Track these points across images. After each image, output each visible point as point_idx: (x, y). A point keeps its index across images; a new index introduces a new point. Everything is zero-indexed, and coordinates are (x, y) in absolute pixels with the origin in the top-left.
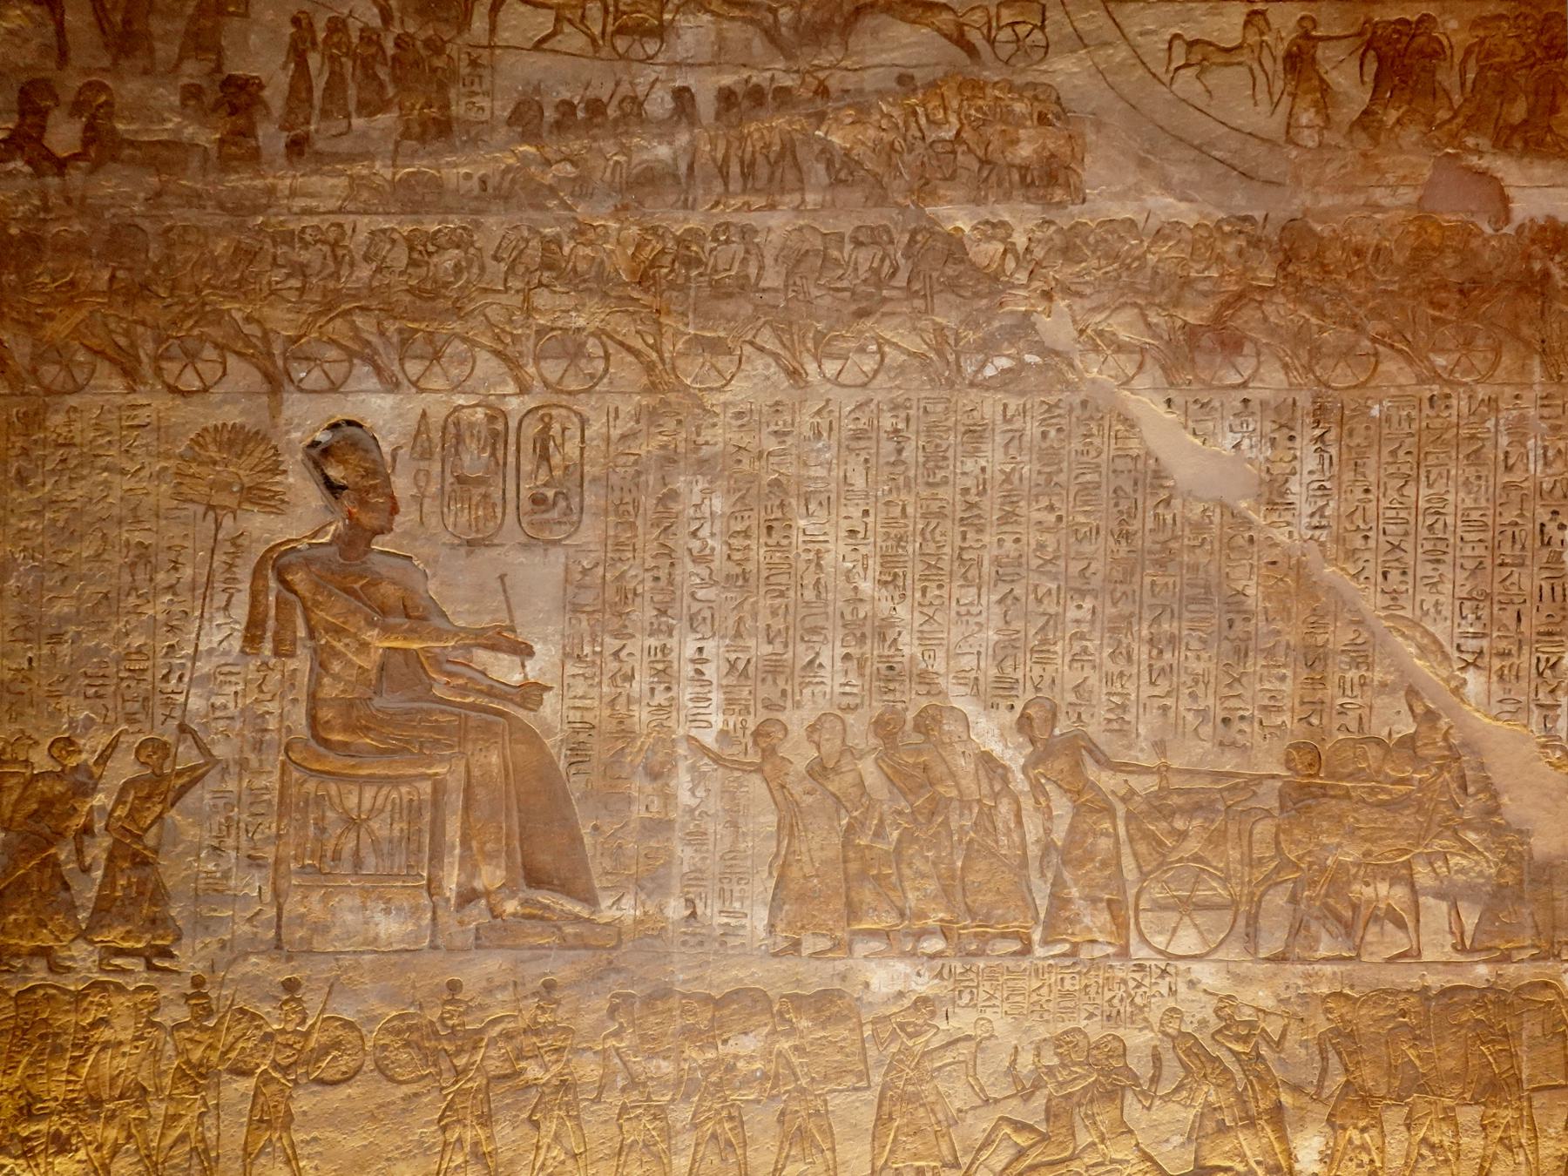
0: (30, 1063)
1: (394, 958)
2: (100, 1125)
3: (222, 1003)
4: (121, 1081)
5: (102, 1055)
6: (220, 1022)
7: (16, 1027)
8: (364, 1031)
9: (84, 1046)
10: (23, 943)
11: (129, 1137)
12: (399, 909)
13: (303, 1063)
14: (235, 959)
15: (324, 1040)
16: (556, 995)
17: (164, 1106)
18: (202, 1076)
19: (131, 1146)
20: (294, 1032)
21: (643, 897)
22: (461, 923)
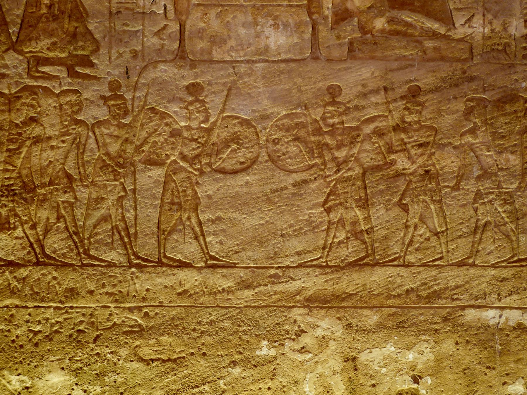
1: (283, 66)
3: (136, 105)
4: (50, 170)
5: (34, 148)
6: (135, 120)
8: (259, 128)
11: (59, 218)
12: (286, 26)
13: (206, 154)
14: (146, 66)
15: (223, 135)
16: (422, 99)
17: (87, 191)
18: (121, 166)
19: (62, 225)
20: (199, 128)
21: (490, 17)
22: (338, 37)
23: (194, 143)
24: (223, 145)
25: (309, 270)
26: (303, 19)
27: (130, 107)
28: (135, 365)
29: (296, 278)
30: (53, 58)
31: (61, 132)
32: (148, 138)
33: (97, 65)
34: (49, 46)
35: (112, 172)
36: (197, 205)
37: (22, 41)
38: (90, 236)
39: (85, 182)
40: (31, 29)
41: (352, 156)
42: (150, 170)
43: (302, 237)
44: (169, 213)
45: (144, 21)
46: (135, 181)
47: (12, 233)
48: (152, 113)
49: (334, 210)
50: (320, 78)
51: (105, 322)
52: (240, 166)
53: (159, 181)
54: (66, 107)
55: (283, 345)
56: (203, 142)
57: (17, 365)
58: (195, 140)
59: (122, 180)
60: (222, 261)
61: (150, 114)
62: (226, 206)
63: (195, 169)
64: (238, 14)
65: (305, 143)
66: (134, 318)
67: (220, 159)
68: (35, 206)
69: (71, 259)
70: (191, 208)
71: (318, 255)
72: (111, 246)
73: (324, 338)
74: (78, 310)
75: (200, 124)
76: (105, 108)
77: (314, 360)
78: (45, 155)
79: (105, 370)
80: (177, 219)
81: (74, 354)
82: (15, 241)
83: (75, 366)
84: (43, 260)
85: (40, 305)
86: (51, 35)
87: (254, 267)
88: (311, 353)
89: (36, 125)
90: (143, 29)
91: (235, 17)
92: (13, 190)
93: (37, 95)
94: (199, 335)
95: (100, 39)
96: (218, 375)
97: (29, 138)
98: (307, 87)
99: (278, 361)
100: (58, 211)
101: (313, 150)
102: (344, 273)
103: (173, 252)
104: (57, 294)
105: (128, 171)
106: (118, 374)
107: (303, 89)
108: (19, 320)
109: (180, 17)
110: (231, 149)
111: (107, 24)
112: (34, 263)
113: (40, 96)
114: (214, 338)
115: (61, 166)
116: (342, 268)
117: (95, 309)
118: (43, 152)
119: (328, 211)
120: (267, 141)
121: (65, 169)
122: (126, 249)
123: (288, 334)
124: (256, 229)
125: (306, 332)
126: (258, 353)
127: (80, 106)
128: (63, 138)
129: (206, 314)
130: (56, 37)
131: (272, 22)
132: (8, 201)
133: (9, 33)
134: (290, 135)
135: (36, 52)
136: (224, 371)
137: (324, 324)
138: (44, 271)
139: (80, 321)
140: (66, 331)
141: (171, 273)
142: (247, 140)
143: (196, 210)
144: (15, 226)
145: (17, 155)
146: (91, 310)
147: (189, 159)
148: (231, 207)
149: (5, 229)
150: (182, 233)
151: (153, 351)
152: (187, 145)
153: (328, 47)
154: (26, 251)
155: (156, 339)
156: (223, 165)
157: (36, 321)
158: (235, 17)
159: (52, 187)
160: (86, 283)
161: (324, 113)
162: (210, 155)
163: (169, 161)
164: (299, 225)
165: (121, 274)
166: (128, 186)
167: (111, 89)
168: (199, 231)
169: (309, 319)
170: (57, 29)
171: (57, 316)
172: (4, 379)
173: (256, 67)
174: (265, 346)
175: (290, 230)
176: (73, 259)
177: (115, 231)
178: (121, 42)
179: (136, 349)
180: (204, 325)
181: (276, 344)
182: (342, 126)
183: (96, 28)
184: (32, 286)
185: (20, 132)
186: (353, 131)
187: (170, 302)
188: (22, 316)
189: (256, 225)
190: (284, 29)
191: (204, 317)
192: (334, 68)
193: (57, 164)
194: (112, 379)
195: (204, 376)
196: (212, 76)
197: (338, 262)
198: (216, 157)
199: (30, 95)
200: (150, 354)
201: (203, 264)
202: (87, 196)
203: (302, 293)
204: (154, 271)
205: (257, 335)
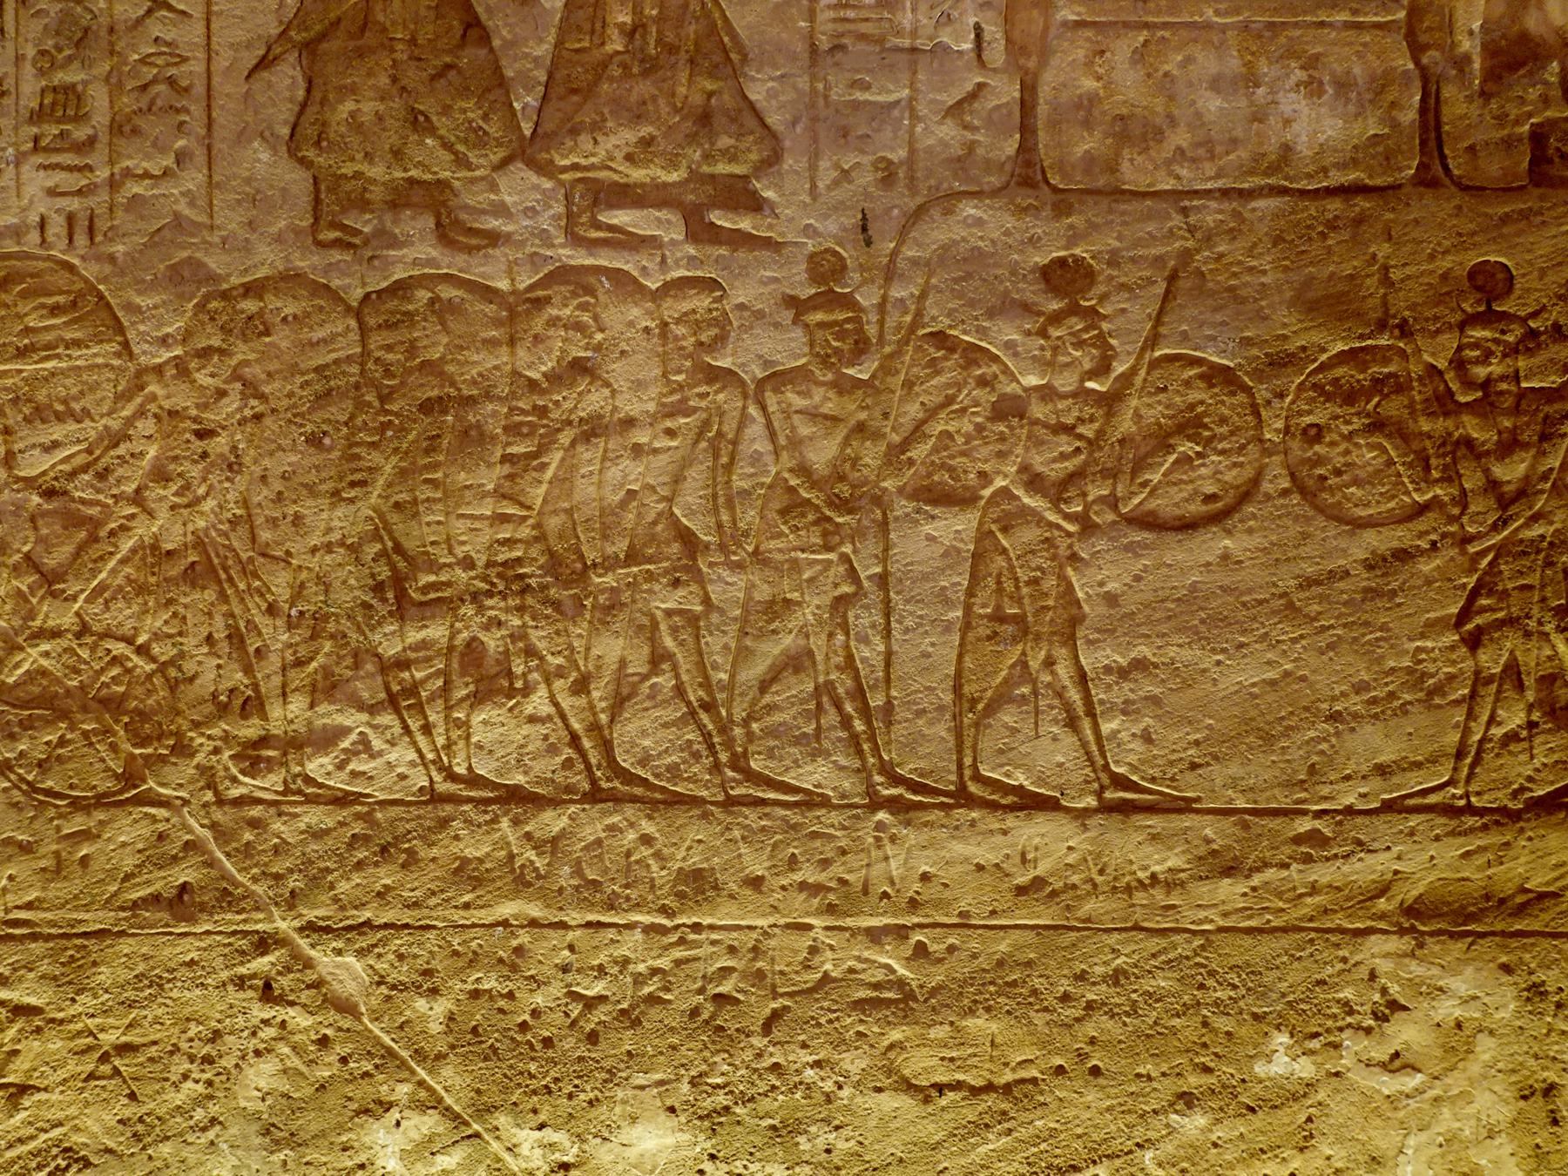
0: (403, 473)
1: (1334, 206)
2: (581, 629)
3: (890, 323)
5: (584, 453)
7: (366, 380)
8: (1262, 392)
9: (538, 429)
10: (376, 171)
11: (658, 659)
12: (1343, 86)
17: (739, 580)
18: (844, 505)
19: (665, 681)
20: (1081, 394)
22: (1501, 119)
23: (1064, 438)
24: (1153, 442)
25: (1414, 821)
26: (1394, 64)
27: (872, 331)
28: (890, 1102)
29: (1376, 845)
30: (643, 185)
31: (664, 405)
32: (924, 422)
33: (772, 206)
34: (631, 150)
35: (816, 523)
36: (1075, 621)
37: (550, 136)
38: (749, 715)
39: (735, 553)
40: (575, 98)
41: (1544, 477)
42: (933, 517)
43: (1393, 722)
44: (989, 647)
45: (915, 73)
46: (886, 550)
47: (518, 703)
48: (938, 349)
49: (1491, 640)
50: (1447, 243)
51: (797, 972)
52: (1204, 508)
53: (959, 551)
54: (681, 330)
55: (1336, 1046)
56: (1090, 434)
57: (535, 1098)
58: (1069, 430)
59: (847, 549)
60: (1151, 792)
61: (932, 350)
62: (1164, 628)
63: (1067, 517)
64: (1197, 51)
65: (1402, 434)
66: (884, 960)
67: (1144, 484)
68: (585, 625)
69: (696, 782)
70: (1054, 633)
71: (1442, 776)
72: (814, 747)
73: (1459, 1026)
74: (714, 936)
75: (1082, 381)
76: (798, 333)
77: (1431, 1093)
78: (614, 473)
79: (799, 1115)
80: (1013, 666)
81: (704, 1067)
82: (527, 729)
83: (708, 1104)
84: (610, 785)
85: (603, 919)
86: (638, 116)
87: (1245, 811)
88: (1419, 1071)
89: (590, 383)
90: (911, 99)
91: (1189, 60)
92: (522, 577)
93: (596, 297)
94: (1079, 1013)
95: (782, 128)
96: (1139, 1134)
97: (569, 423)
98: (1408, 271)
99: (1321, 1096)
100: (653, 640)
101: (1427, 460)
102: (1522, 830)
103: (1002, 766)
104: (653, 887)
105: (865, 522)
106: (837, 1128)
107: (1395, 275)
108: (540, 962)
109: (1022, 61)
110: (1175, 456)
111: (803, 83)
112: (585, 794)
113: (602, 298)
114: (1125, 1024)
115: (661, 506)
116: (1515, 816)
117: (766, 933)
118: (608, 464)
119: (1474, 642)
120: (1287, 430)
121: (672, 514)
122: (860, 752)
123: (1351, 1012)
124: (1256, 696)
125: (1405, 1008)
126: (1260, 1069)
127: (723, 328)
128: (669, 424)
129: (1099, 951)
130: (652, 123)
131: (1300, 75)
132: (507, 610)
133: (513, 113)
134: (1358, 414)
135: (592, 167)
136: (1157, 1123)
137: (1459, 985)
138: (616, 819)
139: (721, 969)
140: (682, 998)
141: (997, 826)
142: (1224, 429)
143: (1070, 640)
144: (526, 682)
145: (534, 474)
146: (755, 936)
147: (1047, 484)
148: (1179, 631)
149: (499, 691)
150: (1031, 708)
151: (942, 1059)
152: (1043, 443)
153: (1471, 149)
154: (559, 760)
155: (952, 1023)
156: (1152, 504)
157: (592, 968)
158: (1189, 60)
159: (635, 569)
160: (740, 856)
161: (1460, 349)
162: (1111, 474)
163: (987, 492)
164: (1387, 684)
165: (844, 828)
166: (867, 568)
167: (816, 276)
168: (1079, 703)
169: (1416, 969)
170: (654, 98)
171: (653, 954)
172: (498, 1138)
173: (1254, 210)
174: (1282, 1049)
175: (1357, 699)
176: (699, 781)
177: (825, 699)
178: (844, 136)
179: (892, 1055)
180: (1094, 984)
181: (1315, 1044)
182: (1514, 388)
183: (772, 94)
184: (579, 862)
185: (541, 403)
186: (1550, 401)
187: (993, 913)
188: (549, 951)
189: (1254, 685)
190: (1337, 95)
191: (1096, 960)
192: (1490, 211)
193: (650, 499)
194: (821, 1143)
195: (1095, 1137)
196: (1119, 238)
197: (1501, 798)
198: (1132, 480)
199: (575, 294)
200: (933, 1069)
201: (1091, 801)
202: (741, 595)
203: (1395, 889)
204: (944, 821)
205: (1255, 1017)
